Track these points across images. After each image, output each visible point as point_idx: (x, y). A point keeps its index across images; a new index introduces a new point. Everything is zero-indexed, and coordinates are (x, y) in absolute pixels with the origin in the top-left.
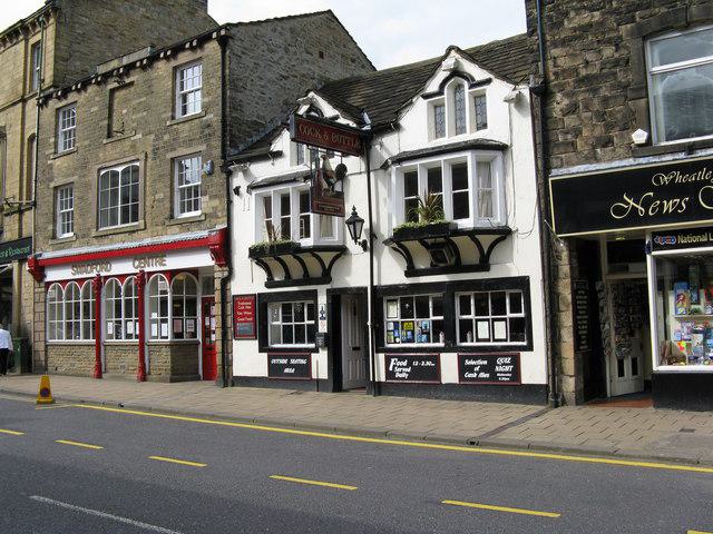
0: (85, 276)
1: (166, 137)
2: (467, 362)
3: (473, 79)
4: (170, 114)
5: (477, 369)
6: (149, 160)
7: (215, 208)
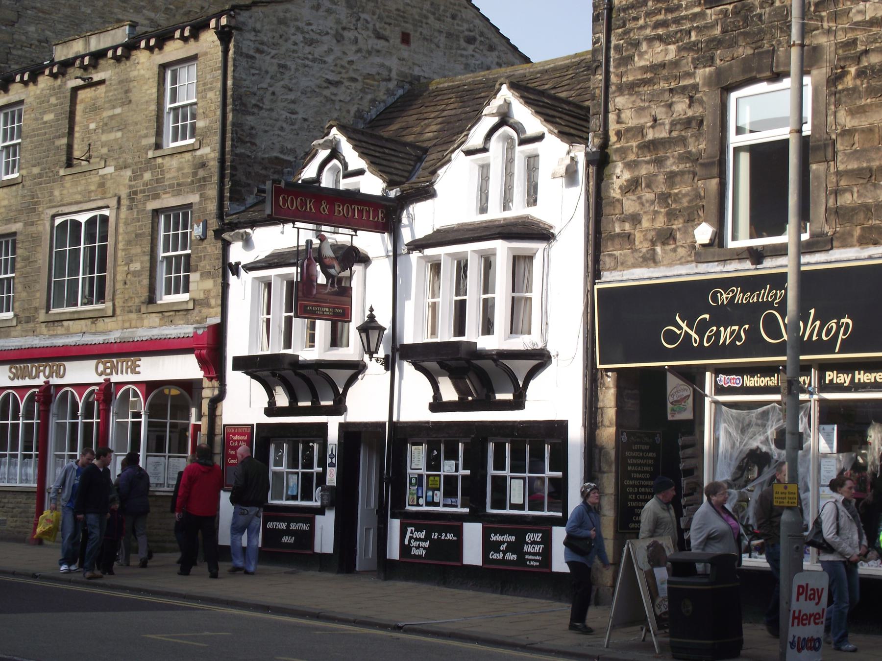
0: (27, 382)
1: (147, 176)
2: (494, 538)
3: (524, 131)
4: (152, 140)
5: (503, 547)
6: (124, 209)
7: (207, 292)
